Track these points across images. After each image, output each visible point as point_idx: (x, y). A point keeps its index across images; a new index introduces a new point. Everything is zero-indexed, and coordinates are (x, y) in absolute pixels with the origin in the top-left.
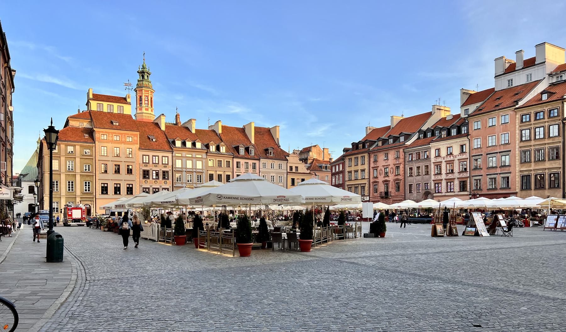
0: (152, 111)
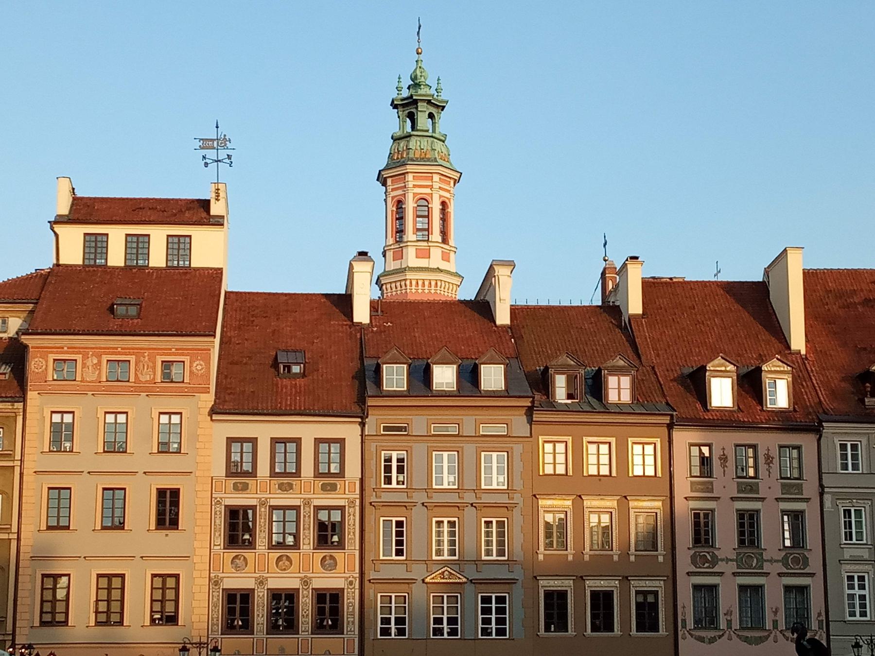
0: (446, 258)
